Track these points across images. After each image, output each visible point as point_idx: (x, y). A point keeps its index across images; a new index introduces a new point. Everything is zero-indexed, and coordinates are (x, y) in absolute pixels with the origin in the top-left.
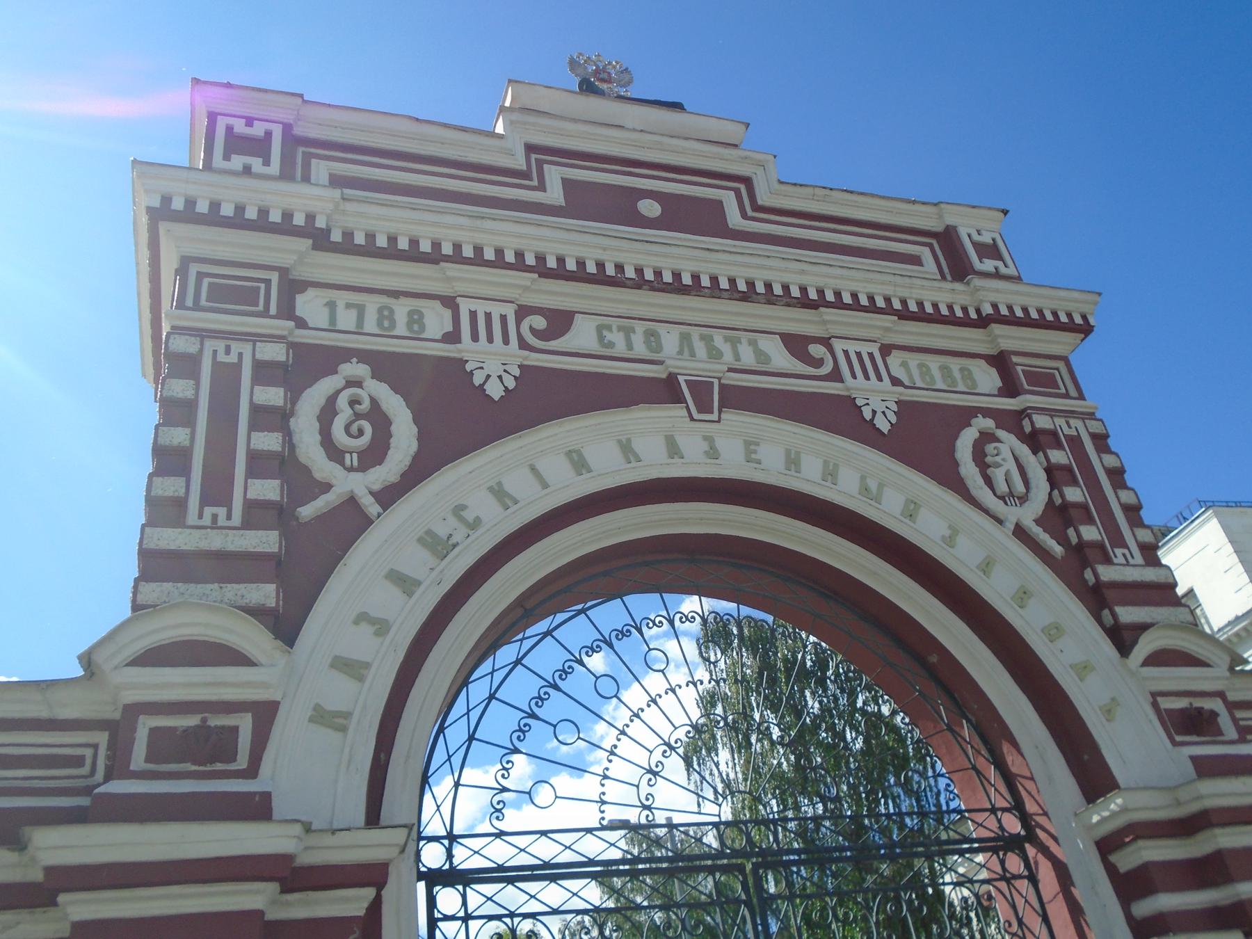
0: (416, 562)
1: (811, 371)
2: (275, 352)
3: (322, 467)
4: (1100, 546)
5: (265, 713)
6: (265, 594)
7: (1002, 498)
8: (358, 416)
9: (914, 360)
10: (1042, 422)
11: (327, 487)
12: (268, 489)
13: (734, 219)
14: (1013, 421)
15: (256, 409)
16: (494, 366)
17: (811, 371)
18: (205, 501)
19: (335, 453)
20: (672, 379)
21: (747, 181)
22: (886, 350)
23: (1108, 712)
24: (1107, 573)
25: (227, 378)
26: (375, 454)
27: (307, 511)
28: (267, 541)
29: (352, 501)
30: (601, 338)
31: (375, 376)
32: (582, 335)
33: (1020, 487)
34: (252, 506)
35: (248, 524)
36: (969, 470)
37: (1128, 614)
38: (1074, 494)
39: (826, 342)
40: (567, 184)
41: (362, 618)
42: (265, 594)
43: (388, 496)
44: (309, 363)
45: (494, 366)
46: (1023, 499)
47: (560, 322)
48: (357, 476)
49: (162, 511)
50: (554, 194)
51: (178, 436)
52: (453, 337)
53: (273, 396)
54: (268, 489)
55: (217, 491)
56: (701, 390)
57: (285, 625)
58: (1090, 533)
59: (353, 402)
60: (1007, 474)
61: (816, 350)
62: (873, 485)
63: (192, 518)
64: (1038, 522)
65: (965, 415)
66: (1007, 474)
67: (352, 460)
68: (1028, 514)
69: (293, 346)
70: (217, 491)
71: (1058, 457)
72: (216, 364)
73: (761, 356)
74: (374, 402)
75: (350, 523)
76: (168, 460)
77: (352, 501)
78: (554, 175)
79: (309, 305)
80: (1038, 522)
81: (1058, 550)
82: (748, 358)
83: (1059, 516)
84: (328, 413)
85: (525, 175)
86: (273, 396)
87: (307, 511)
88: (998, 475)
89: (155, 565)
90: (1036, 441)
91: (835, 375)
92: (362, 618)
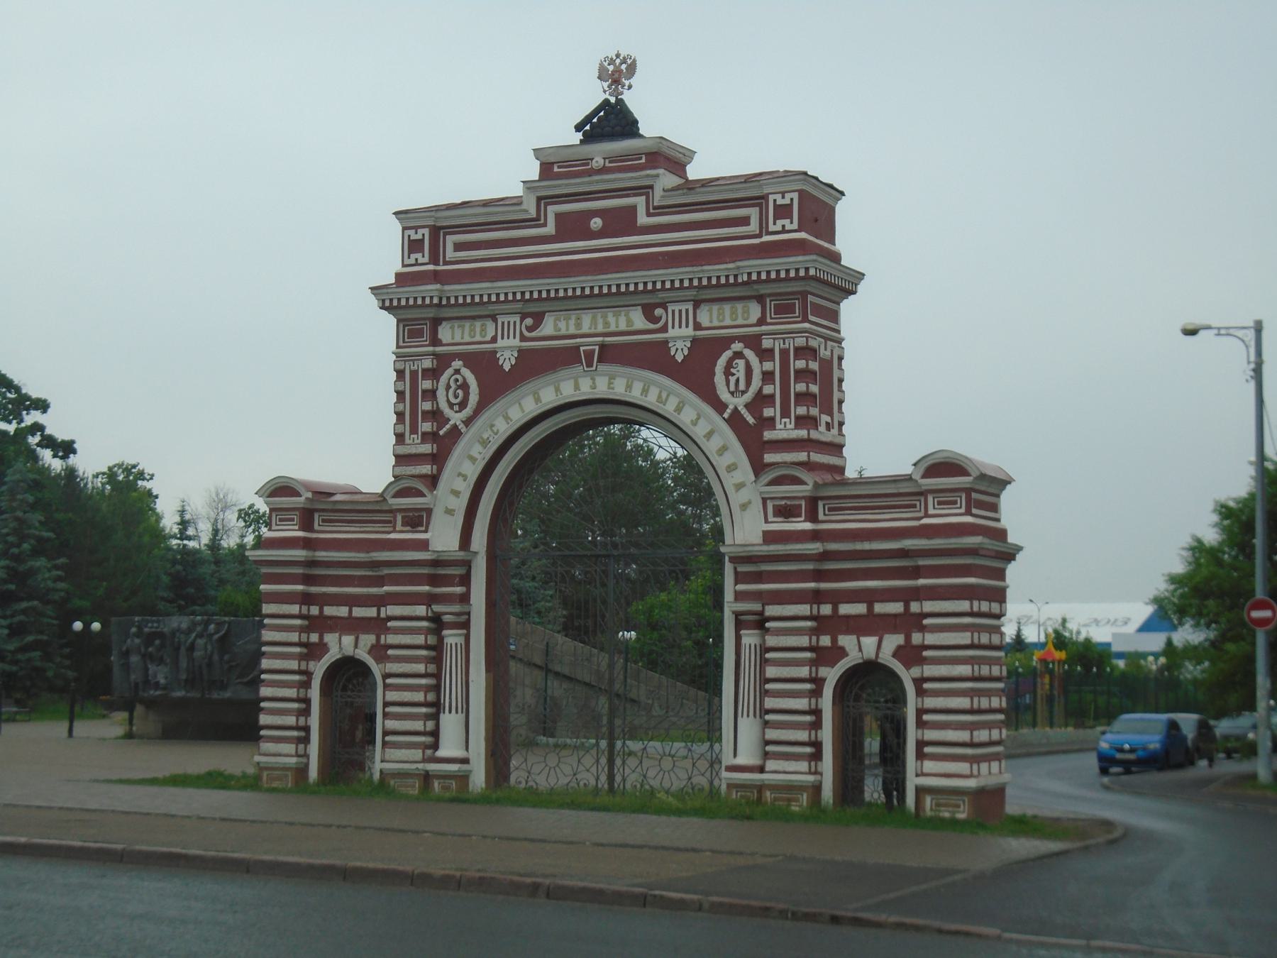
0: (477, 450)
1: (652, 326)
2: (427, 363)
3: (447, 411)
4: (772, 419)
5: (429, 511)
6: (426, 469)
7: (732, 393)
8: (459, 387)
9: (715, 308)
10: (767, 343)
11: (449, 420)
12: (426, 427)
13: (642, 219)
14: (753, 342)
15: (424, 392)
16: (507, 352)
17: (652, 326)
18: (411, 433)
19: (451, 405)
20: (577, 348)
21: (651, 187)
22: (697, 304)
23: (744, 507)
24: (768, 435)
25: (414, 374)
26: (463, 405)
27: (441, 433)
28: (427, 448)
29: (455, 426)
30: (555, 325)
31: (465, 366)
32: (548, 328)
33: (742, 386)
34: (424, 434)
35: (423, 441)
36: (719, 379)
37: (769, 458)
38: (768, 390)
39: (664, 306)
40: (558, 216)
41: (460, 474)
42: (426, 469)
43: (468, 422)
44: (443, 361)
45: (507, 352)
46: (743, 392)
47: (539, 318)
48: (458, 415)
49: (400, 438)
50: (550, 229)
51: (401, 407)
52: (494, 340)
53: (427, 384)
54: (426, 427)
55: (414, 430)
56: (589, 355)
57: (433, 481)
58: (768, 412)
59: (457, 380)
60: (738, 380)
61: (659, 311)
62: (664, 395)
63: (407, 441)
64: (746, 406)
65: (726, 342)
66: (738, 380)
67: (456, 408)
68: (739, 402)
69: (435, 355)
70: (414, 430)
71: (768, 366)
72: (411, 372)
73: (629, 322)
74: (464, 379)
75: (455, 434)
76: (400, 416)
77: (455, 426)
78: (552, 210)
79: (446, 333)
80: (746, 406)
81: (751, 420)
82: (623, 326)
83: (761, 400)
84: (448, 387)
85: (538, 219)
86: (427, 384)
87: (441, 433)
88: (733, 379)
89: (401, 459)
90: (765, 354)
91: (664, 329)
92: (460, 474)
